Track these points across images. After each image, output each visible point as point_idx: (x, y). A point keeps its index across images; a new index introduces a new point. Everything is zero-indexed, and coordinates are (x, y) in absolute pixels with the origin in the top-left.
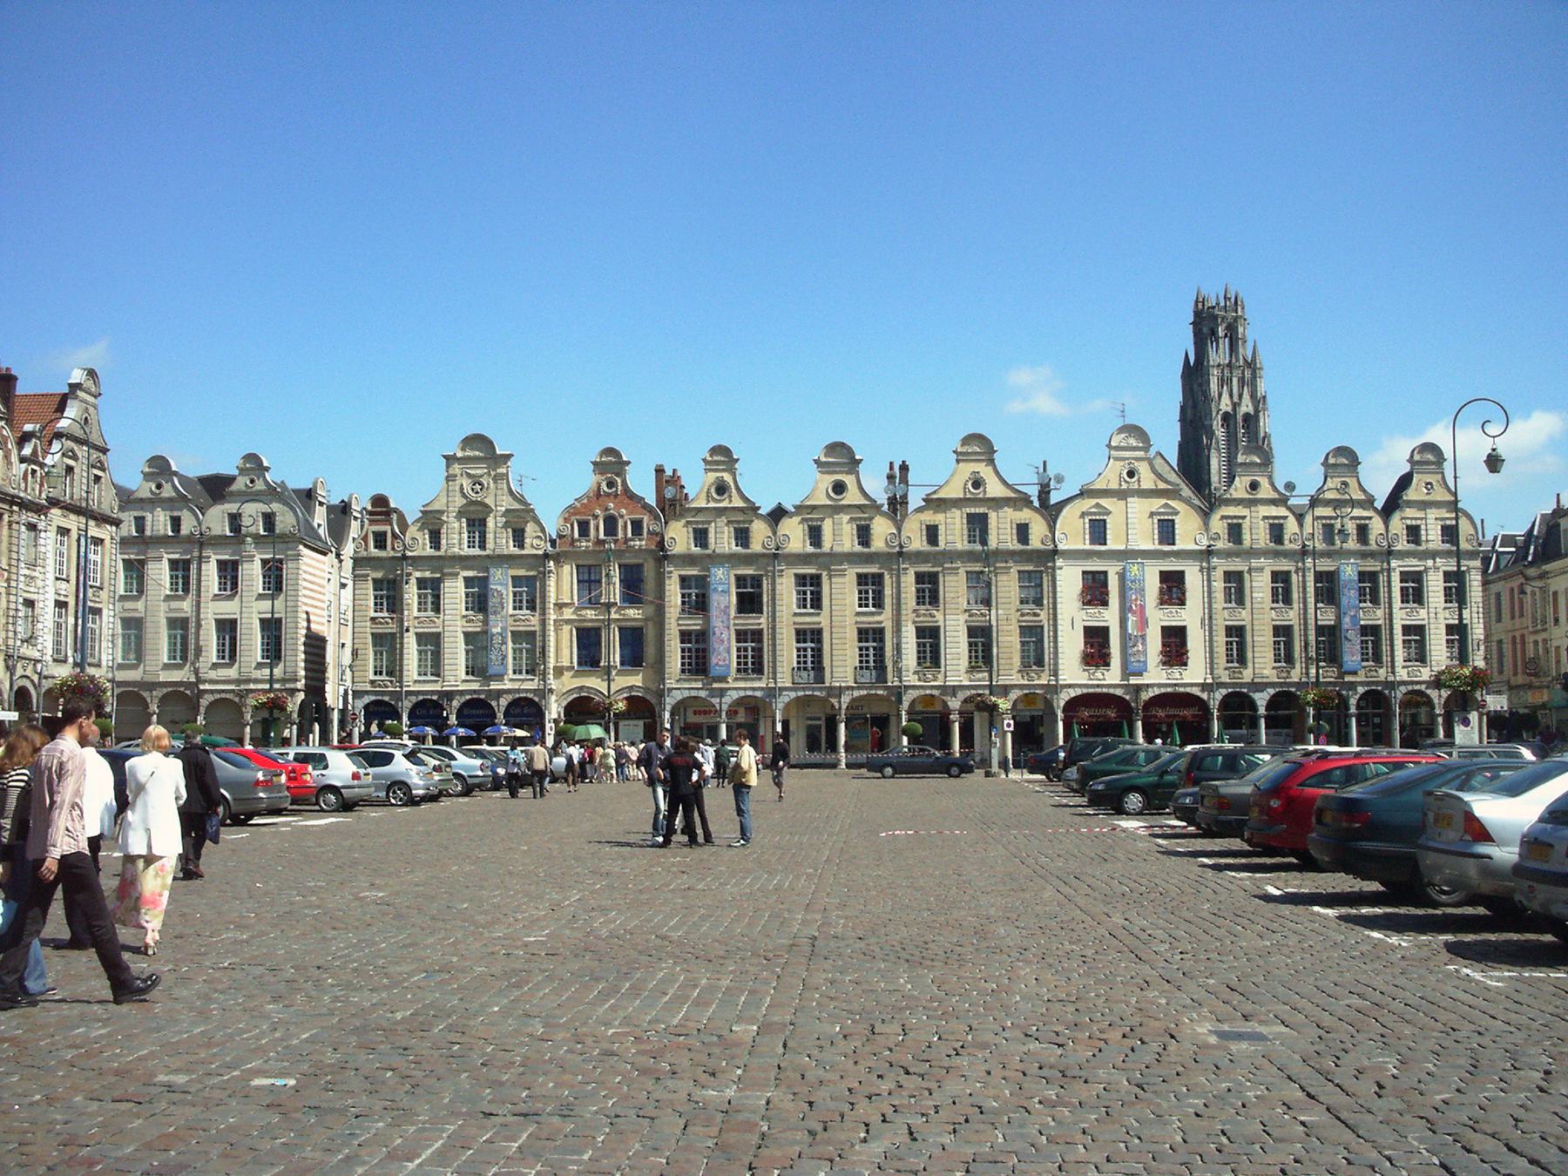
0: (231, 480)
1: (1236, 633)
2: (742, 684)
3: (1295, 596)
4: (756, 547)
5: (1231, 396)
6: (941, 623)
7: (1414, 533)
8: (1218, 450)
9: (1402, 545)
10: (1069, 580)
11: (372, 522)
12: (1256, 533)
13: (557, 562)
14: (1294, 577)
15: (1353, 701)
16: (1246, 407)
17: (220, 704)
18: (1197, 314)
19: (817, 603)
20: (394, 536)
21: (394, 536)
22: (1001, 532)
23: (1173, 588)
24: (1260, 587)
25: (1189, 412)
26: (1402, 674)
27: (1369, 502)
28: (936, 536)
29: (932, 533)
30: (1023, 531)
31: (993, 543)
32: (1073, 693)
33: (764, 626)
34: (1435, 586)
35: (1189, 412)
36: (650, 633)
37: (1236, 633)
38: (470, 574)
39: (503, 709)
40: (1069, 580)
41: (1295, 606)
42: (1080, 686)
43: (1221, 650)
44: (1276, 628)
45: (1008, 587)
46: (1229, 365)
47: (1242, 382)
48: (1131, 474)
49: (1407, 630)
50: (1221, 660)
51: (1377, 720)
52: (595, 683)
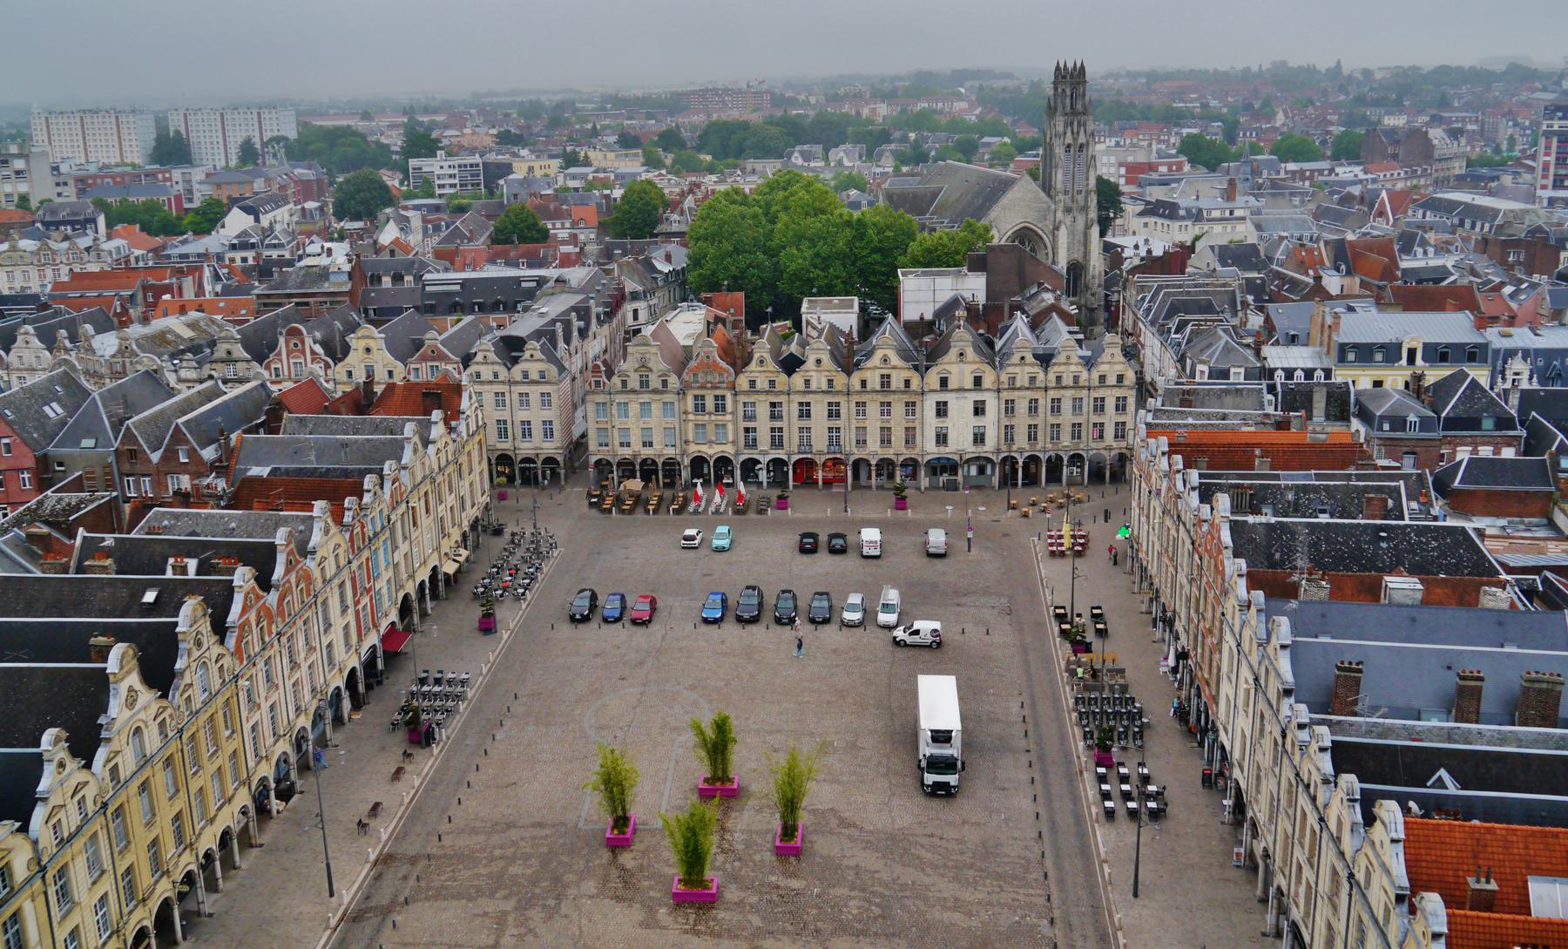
1: (1009, 429)
3: (1040, 410)
4: (778, 388)
7: (1102, 378)
12: (1021, 380)
15: (1065, 459)
17: (527, 460)
19: (809, 416)
22: (897, 382)
23: (979, 410)
24: (1022, 407)
26: (1093, 445)
29: (864, 383)
30: (907, 383)
31: (893, 387)
34: (1110, 404)
36: (730, 427)
37: (1009, 429)
45: (898, 409)
49: (1095, 425)
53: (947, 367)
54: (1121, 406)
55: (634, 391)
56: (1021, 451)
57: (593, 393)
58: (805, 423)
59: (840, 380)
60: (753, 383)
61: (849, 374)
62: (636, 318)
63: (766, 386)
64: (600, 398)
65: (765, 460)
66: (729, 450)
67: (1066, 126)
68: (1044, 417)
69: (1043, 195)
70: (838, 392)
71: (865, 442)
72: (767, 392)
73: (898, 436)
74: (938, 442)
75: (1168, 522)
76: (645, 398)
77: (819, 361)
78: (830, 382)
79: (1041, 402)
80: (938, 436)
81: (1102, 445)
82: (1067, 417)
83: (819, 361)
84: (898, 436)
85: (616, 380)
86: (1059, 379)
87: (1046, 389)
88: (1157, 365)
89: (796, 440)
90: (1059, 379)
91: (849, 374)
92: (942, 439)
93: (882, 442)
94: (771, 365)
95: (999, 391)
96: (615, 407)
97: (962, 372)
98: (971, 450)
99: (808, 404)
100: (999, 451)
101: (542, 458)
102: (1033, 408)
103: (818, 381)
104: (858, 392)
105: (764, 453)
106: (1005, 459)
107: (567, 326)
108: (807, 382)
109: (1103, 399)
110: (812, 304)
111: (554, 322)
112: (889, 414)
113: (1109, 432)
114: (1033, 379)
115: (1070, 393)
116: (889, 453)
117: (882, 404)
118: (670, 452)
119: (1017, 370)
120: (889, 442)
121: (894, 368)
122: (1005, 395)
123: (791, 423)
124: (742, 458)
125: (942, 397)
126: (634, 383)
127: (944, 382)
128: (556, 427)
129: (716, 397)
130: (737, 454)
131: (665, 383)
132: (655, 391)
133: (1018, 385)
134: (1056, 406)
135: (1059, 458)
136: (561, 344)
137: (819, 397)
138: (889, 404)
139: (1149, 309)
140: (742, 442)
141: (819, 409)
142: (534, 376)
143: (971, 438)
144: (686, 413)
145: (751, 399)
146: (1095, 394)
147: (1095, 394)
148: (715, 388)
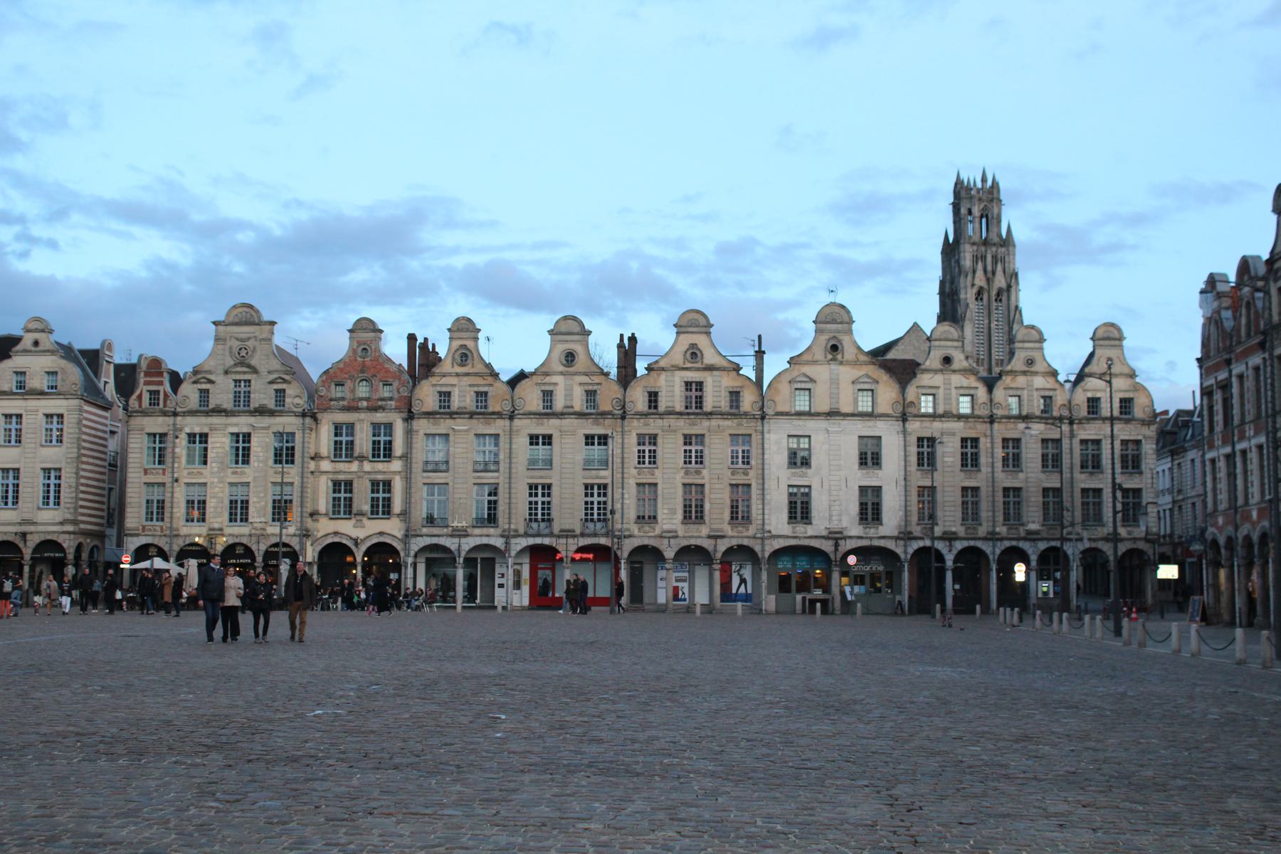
0: (15, 341)
1: (928, 494)
2: (477, 531)
4: (493, 406)
6: (659, 481)
7: (1093, 403)
11: (146, 383)
13: (316, 420)
14: (982, 440)
16: (1000, 282)
18: (957, 194)
20: (166, 395)
24: (949, 453)
25: (947, 285)
27: (1054, 374)
28: (656, 401)
29: (653, 397)
31: (708, 407)
32: (778, 544)
33: (501, 481)
35: (947, 285)
36: (398, 485)
37: (928, 494)
38: (235, 430)
39: (262, 553)
41: (984, 469)
43: (914, 508)
44: (964, 489)
47: (995, 259)
48: (834, 348)
50: (914, 518)
52: (348, 529)
56: (950, 537)
57: (144, 413)
60: (445, 396)
64: (157, 424)
66: (392, 528)
67: (976, 259)
71: (654, 518)
72: (472, 415)
73: (717, 502)
74: (792, 517)
76: (241, 424)
78: (591, 395)
79: (984, 444)
80: (792, 505)
84: (717, 502)
85: (189, 391)
87: (992, 420)
89: (522, 509)
92: (800, 509)
93: (687, 516)
95: (904, 418)
96: (183, 441)
97: (834, 382)
99: (548, 440)
100: (906, 536)
101: (33, 541)
105: (461, 533)
115: (1038, 429)
116: (699, 535)
117: (688, 440)
119: (938, 380)
120: (700, 518)
121: (710, 368)
122: (915, 426)
126: (222, 394)
128: (68, 479)
129: (376, 426)
130: (407, 536)
131: (280, 394)
133: (940, 410)
134: (1013, 460)
137: (567, 423)
138: (700, 438)
142: (37, 381)
143: (854, 509)
144: (316, 457)
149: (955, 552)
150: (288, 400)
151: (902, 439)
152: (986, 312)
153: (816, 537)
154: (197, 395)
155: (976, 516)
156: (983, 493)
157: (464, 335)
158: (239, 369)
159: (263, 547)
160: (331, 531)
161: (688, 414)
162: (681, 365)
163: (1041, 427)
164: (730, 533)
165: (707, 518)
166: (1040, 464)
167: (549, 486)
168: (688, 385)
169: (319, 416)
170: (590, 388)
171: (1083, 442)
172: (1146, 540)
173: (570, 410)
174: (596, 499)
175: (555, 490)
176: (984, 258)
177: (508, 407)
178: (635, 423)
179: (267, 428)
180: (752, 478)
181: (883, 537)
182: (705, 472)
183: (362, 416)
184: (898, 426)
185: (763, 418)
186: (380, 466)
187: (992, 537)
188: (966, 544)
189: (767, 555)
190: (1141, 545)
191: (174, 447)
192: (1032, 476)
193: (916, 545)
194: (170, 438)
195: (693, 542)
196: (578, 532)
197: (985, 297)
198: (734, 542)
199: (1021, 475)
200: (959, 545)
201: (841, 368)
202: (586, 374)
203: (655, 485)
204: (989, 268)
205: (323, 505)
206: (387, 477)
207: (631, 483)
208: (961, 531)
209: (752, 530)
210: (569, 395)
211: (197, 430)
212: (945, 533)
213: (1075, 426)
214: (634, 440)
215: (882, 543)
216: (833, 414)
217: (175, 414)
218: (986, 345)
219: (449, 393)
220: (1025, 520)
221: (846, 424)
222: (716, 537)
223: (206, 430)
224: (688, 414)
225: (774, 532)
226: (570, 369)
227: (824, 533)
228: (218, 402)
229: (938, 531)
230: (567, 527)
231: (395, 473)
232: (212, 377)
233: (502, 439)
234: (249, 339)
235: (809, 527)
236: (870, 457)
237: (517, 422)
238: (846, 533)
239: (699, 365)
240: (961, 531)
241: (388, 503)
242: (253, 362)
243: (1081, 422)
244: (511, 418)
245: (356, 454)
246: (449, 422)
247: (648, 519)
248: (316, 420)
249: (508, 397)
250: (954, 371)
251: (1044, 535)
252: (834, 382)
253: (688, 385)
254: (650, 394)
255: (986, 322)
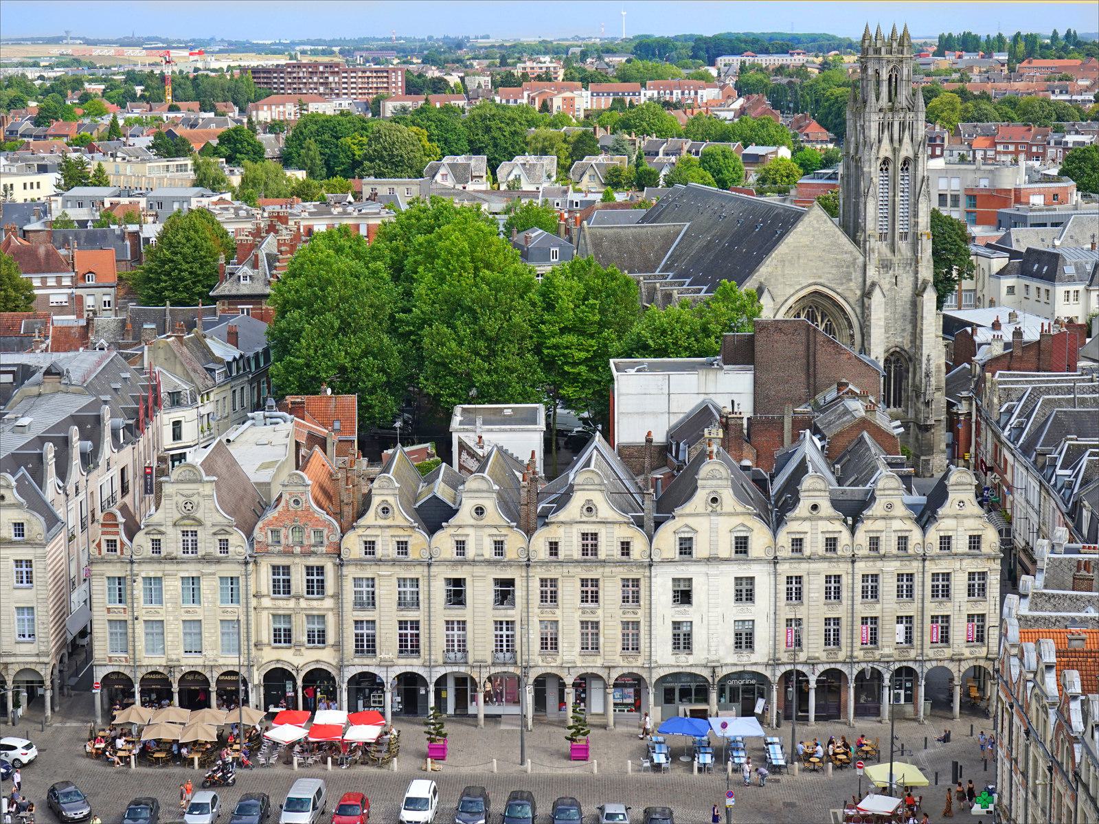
1: (794, 623)
4: (413, 554)
5: (892, 140)
6: (559, 619)
7: (946, 542)
8: (875, 196)
9: (936, 549)
10: (661, 586)
11: (104, 533)
12: (814, 544)
15: (887, 676)
20: (122, 544)
21: (122, 544)
22: (608, 546)
24: (814, 589)
26: (930, 653)
28: (556, 549)
29: (554, 547)
30: (626, 547)
31: (602, 555)
34: (959, 584)
36: (331, 620)
37: (794, 623)
38: (186, 574)
40: (661, 586)
41: (844, 602)
42: (668, 666)
43: (782, 638)
44: (827, 620)
45: (611, 591)
46: (891, 109)
47: (903, 126)
48: (714, 500)
49: (934, 619)
50: (783, 647)
51: (908, 685)
53: (691, 521)
54: (977, 587)
55: (172, 559)
57: (104, 561)
58: (456, 613)
59: (515, 542)
60: (370, 546)
61: (529, 532)
62: (177, 436)
63: (392, 551)
65: (388, 676)
66: (325, 657)
67: (881, 128)
68: (852, 607)
69: (844, 240)
70: (510, 564)
72: (394, 562)
73: (611, 635)
74: (676, 646)
75: (1059, 785)
76: (191, 570)
77: (480, 511)
78: (499, 546)
79: (845, 580)
80: (676, 637)
81: (948, 652)
82: (889, 605)
83: (480, 511)
84: (611, 635)
86: (874, 543)
88: (1034, 518)
89: (440, 643)
90: (874, 543)
91: (529, 532)
92: (683, 640)
94: (400, 517)
97: (713, 530)
98: (729, 659)
100: (775, 662)
102: (833, 590)
103: (480, 544)
104: (543, 563)
106: (787, 676)
107: (63, 444)
108: (461, 545)
109: (947, 576)
110: (469, 421)
111: (41, 440)
112: (595, 598)
113: (960, 631)
114: (831, 544)
116: (594, 664)
117: (584, 582)
118: (231, 661)
119: (806, 526)
123: (435, 612)
124: (350, 673)
125: (683, 571)
126: (173, 543)
127: (686, 547)
132: (207, 559)
134: (871, 590)
135: (877, 675)
136: (52, 479)
137: (478, 570)
139: (1020, 428)
140: (350, 645)
141: (480, 591)
143: (731, 640)
144: (257, 596)
145: (369, 573)
146: (932, 568)
147: (932, 568)
148: (307, 554)
149: (817, 673)
150: (230, 549)
151: (772, 577)
152: (891, 184)
153: (696, 666)
154: (150, 544)
155: (837, 642)
156: (844, 623)
157: (385, 492)
158: (186, 522)
159: (216, 675)
160: (274, 658)
161: (585, 561)
162: (578, 519)
163: (898, 564)
164: (622, 664)
165: (601, 650)
166: (895, 593)
167: (464, 622)
168: (585, 536)
169: (259, 560)
170: (498, 539)
171: (935, 576)
172: (987, 659)
173: (481, 558)
174: (504, 632)
175: (469, 626)
176: (891, 125)
177: (427, 556)
178: (538, 569)
179: (214, 574)
180: (641, 616)
181: (755, 664)
182: (600, 612)
183: (297, 560)
184: (771, 568)
185: (650, 566)
186: (315, 604)
187: (851, 661)
188: (827, 667)
189: (654, 681)
190: (982, 663)
191: (132, 590)
192: (889, 605)
193: (783, 669)
194: (129, 582)
195: (589, 671)
196: (490, 662)
197: (891, 167)
198: (626, 671)
199: (878, 606)
200: (821, 669)
201: (720, 518)
202: (495, 527)
203: (557, 622)
204: (896, 136)
205: (266, 636)
206: (322, 613)
207: (536, 620)
208: (823, 656)
209: (640, 661)
210: (479, 544)
211: (152, 574)
212: (809, 658)
213: (927, 563)
214: (538, 583)
215: (754, 669)
216: (711, 560)
217: (132, 562)
218: (890, 219)
219: (374, 542)
220: (880, 644)
221: (724, 568)
222: (609, 668)
223: (159, 575)
224: (585, 561)
225: (660, 662)
226: (481, 523)
227: (704, 662)
228: (169, 550)
229: (802, 657)
230: (480, 658)
231: (328, 609)
232: (163, 529)
233: (421, 583)
234: (193, 495)
235: (690, 657)
236: (745, 592)
237: (433, 569)
238: (723, 662)
239: (594, 519)
240: (823, 656)
241: (322, 635)
242: (198, 515)
243: (933, 559)
244: (429, 565)
245: (292, 593)
246: (375, 568)
247: (550, 643)
248: (255, 562)
249: (426, 546)
250: (821, 518)
251: (897, 658)
252: (713, 530)
253: (585, 536)
254: (551, 543)
255: (891, 194)
